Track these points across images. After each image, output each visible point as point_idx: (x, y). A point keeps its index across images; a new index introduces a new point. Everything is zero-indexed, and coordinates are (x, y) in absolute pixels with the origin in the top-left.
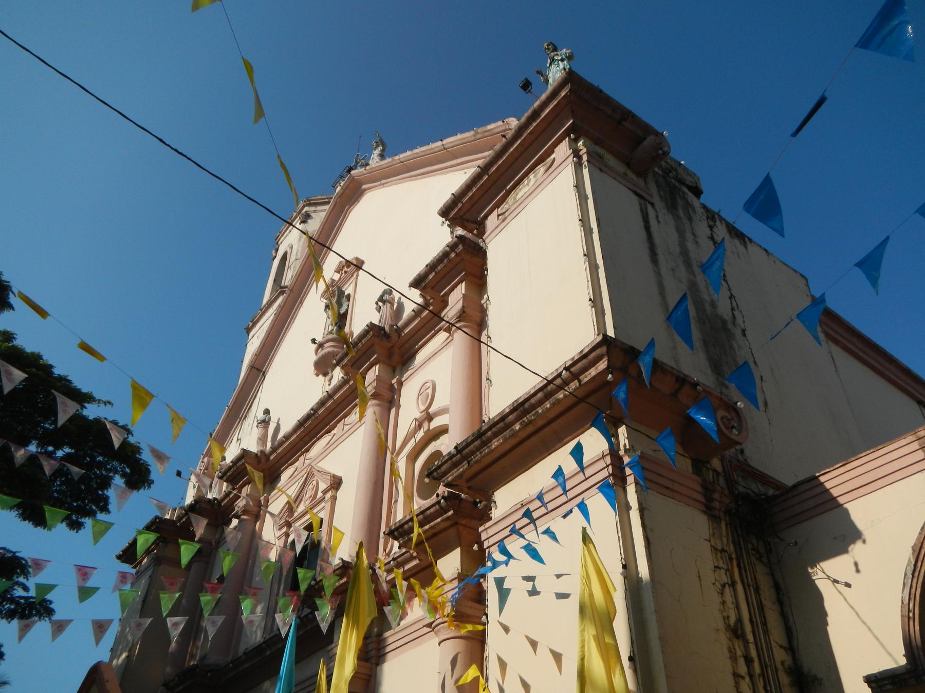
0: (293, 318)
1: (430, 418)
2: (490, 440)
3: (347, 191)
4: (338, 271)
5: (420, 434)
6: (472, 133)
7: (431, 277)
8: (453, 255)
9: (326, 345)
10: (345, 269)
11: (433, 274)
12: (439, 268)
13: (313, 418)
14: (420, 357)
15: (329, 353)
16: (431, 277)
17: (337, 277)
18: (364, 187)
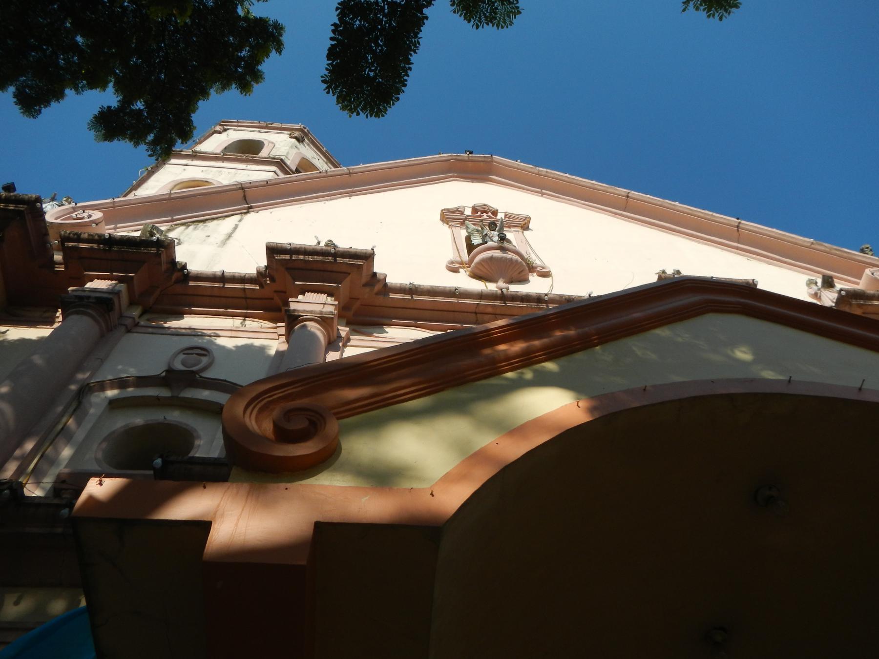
0: (331, 197)
3: (470, 164)
4: (475, 210)
6: (812, 240)
10: (490, 214)
13: (534, 305)
18: (493, 177)
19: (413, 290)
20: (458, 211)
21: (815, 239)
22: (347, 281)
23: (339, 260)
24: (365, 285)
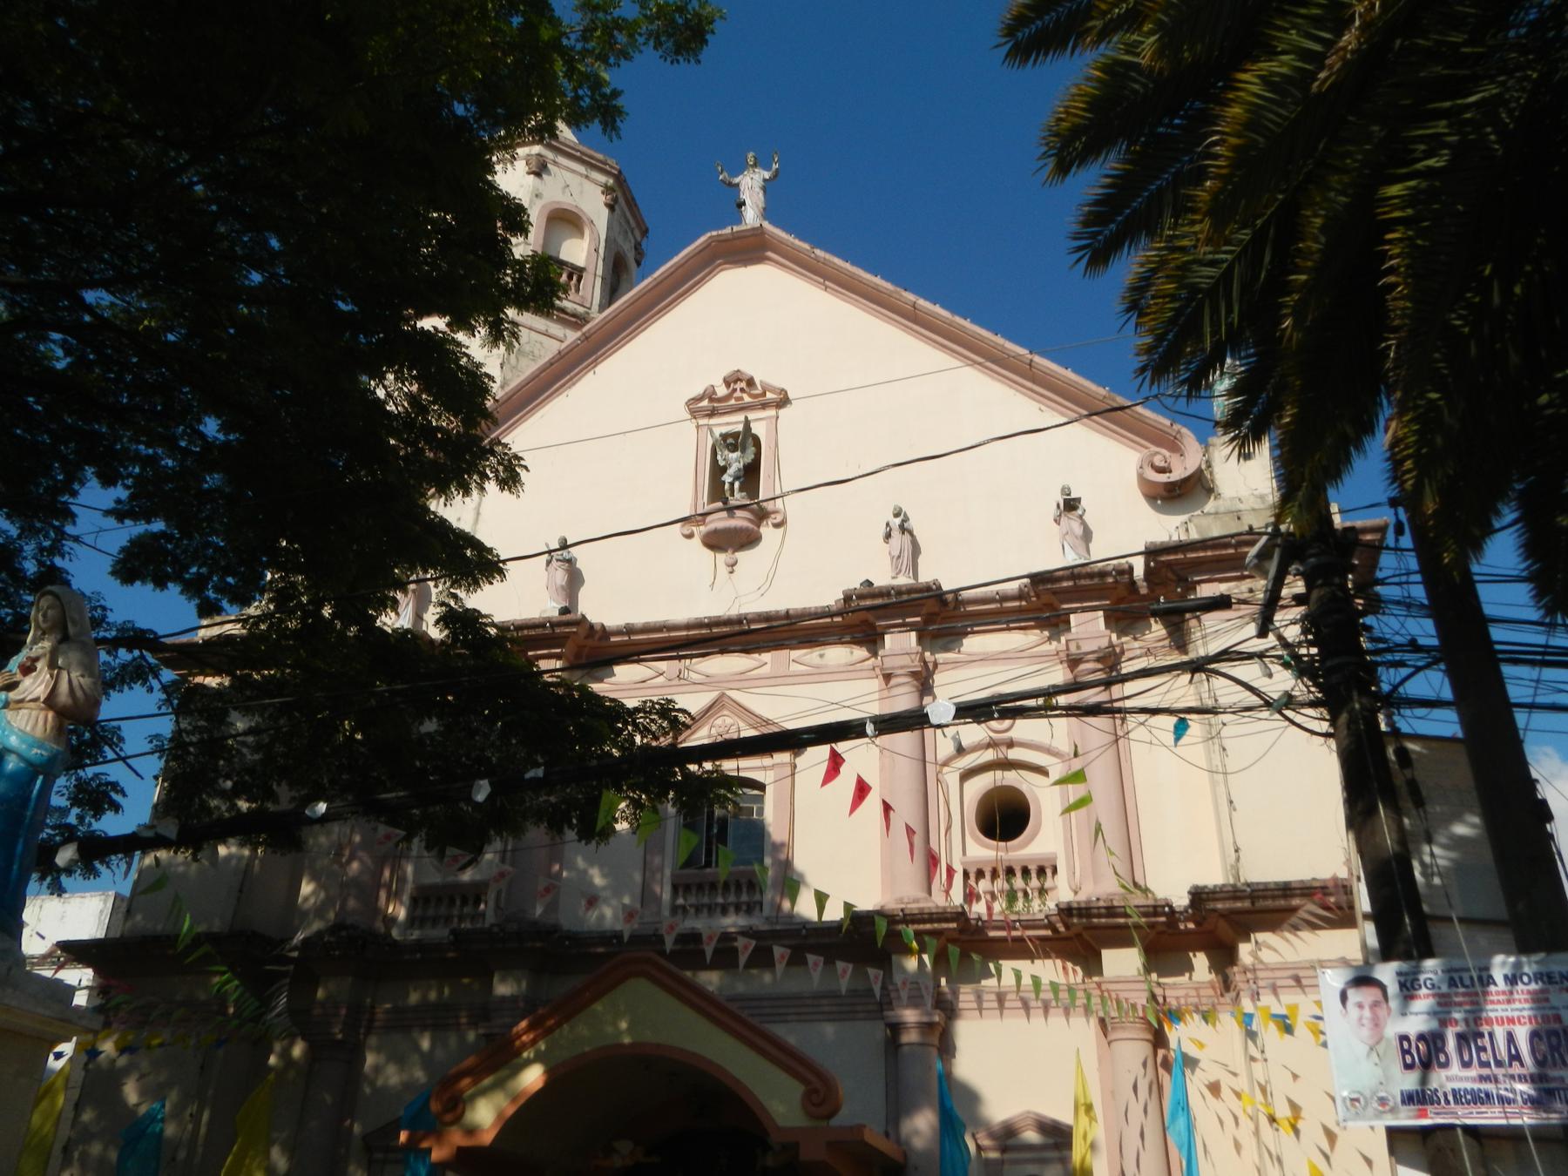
0: (572, 382)
1: (1011, 744)
2: (1293, 896)
4: (727, 383)
5: (989, 755)
7: (1065, 584)
8: (1110, 580)
9: (739, 513)
10: (743, 385)
11: (1071, 583)
12: (1083, 582)
14: (972, 644)
15: (747, 529)
16: (1065, 584)
17: (722, 391)
18: (770, 254)
19: (630, 630)
20: (710, 394)
21: (1112, 390)
22: (570, 643)
23: (557, 630)
24: (586, 637)
